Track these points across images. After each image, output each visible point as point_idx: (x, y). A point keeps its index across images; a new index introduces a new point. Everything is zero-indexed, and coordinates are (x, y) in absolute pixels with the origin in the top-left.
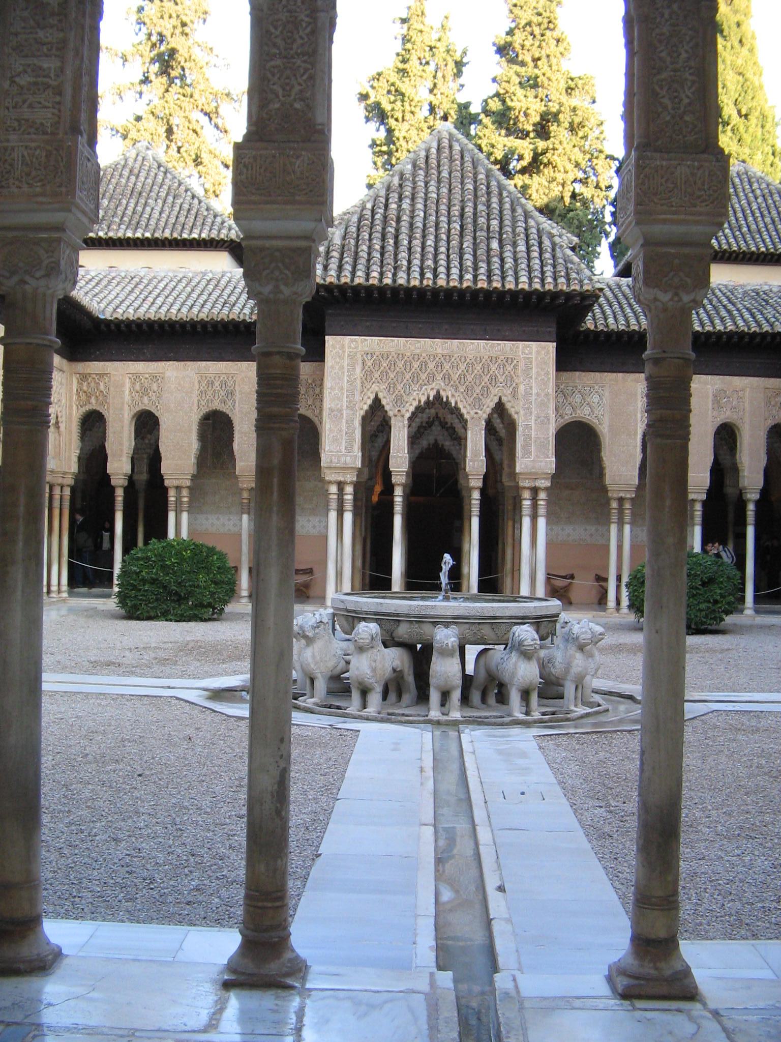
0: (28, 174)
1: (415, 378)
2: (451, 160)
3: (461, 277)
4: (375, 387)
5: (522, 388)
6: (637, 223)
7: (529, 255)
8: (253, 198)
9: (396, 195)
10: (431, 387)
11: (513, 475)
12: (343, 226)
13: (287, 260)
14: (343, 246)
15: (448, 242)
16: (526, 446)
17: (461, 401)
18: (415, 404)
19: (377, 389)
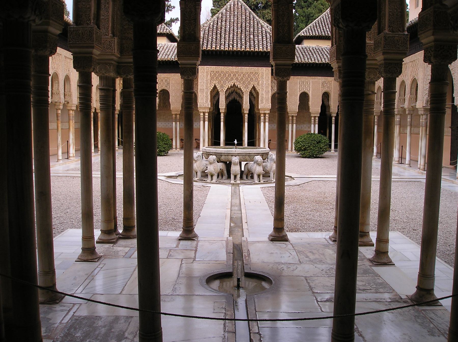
0: (128, 50)
1: (227, 79)
2: (238, 9)
3: (241, 47)
4: (214, 82)
5: (260, 82)
6: (273, 61)
7: (262, 40)
8: (182, 55)
9: (220, 20)
10: (232, 82)
11: (259, 110)
12: (204, 31)
13: (190, 70)
14: (204, 37)
15: (237, 36)
16: (262, 101)
17: (242, 86)
18: (227, 87)
19: (215, 82)
